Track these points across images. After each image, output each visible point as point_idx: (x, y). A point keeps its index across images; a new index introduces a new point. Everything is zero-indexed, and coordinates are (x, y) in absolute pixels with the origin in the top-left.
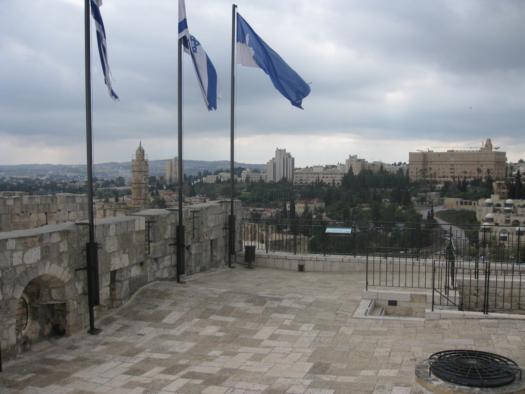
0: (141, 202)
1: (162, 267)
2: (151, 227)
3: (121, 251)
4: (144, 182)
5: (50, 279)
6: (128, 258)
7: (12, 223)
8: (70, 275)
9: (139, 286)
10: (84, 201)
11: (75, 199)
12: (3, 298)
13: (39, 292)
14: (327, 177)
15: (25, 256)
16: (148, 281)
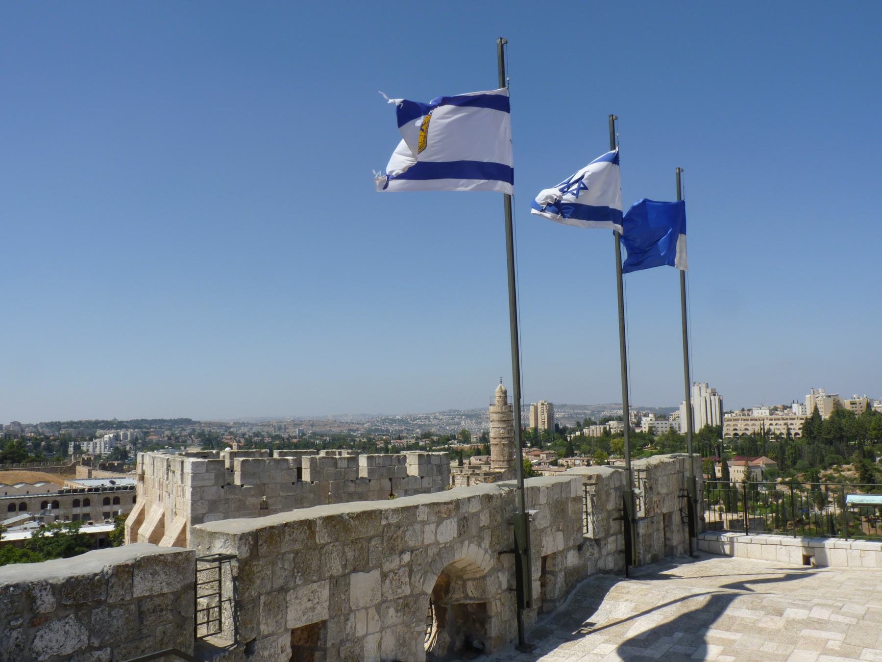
1: (606, 554)
5: (465, 567)
9: (578, 581)
12: (412, 591)
14: (776, 424)
16: (588, 574)
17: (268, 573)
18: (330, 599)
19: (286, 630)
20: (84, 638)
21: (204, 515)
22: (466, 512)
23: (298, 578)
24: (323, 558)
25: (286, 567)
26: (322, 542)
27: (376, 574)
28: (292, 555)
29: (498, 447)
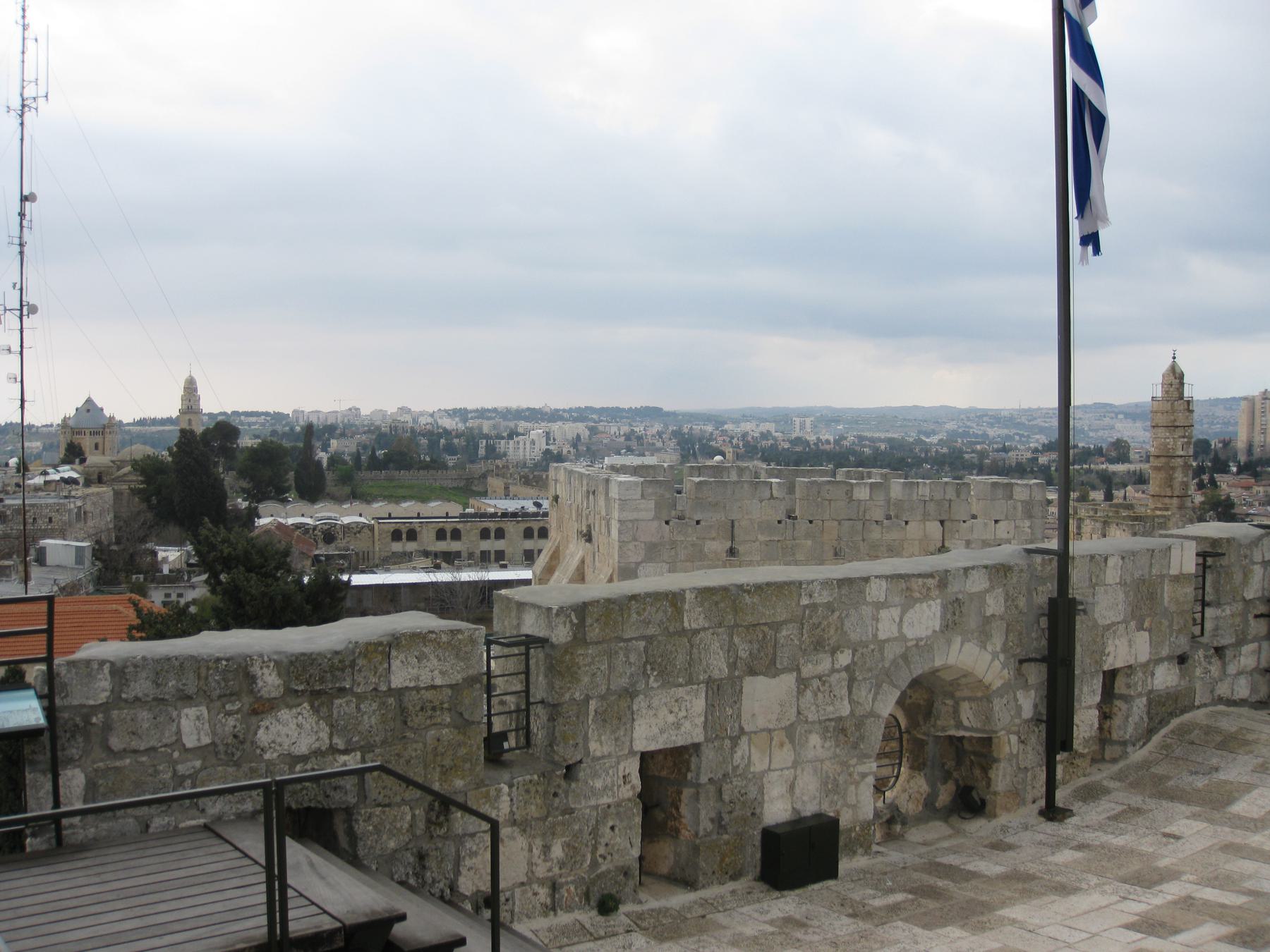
0: (1171, 504)
1: (1234, 672)
2: (1210, 567)
3: (1133, 624)
4: (1181, 453)
5: (958, 679)
6: (1148, 643)
7: (863, 540)
8: (1006, 671)
9: (1172, 715)
10: (1033, 496)
11: (1012, 492)
12: (852, 711)
13: (930, 704)
15: (905, 619)
16: (1196, 704)
17: (602, 668)
18: (706, 712)
19: (632, 752)
20: (324, 736)
21: (638, 564)
22: (960, 592)
23: (652, 679)
24: (695, 650)
25: (632, 660)
26: (694, 626)
27: (789, 680)
28: (642, 644)
29: (1162, 472)
